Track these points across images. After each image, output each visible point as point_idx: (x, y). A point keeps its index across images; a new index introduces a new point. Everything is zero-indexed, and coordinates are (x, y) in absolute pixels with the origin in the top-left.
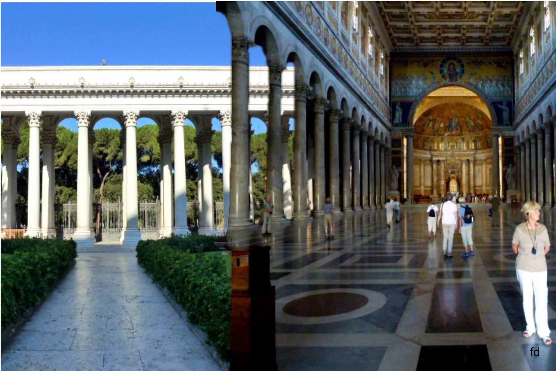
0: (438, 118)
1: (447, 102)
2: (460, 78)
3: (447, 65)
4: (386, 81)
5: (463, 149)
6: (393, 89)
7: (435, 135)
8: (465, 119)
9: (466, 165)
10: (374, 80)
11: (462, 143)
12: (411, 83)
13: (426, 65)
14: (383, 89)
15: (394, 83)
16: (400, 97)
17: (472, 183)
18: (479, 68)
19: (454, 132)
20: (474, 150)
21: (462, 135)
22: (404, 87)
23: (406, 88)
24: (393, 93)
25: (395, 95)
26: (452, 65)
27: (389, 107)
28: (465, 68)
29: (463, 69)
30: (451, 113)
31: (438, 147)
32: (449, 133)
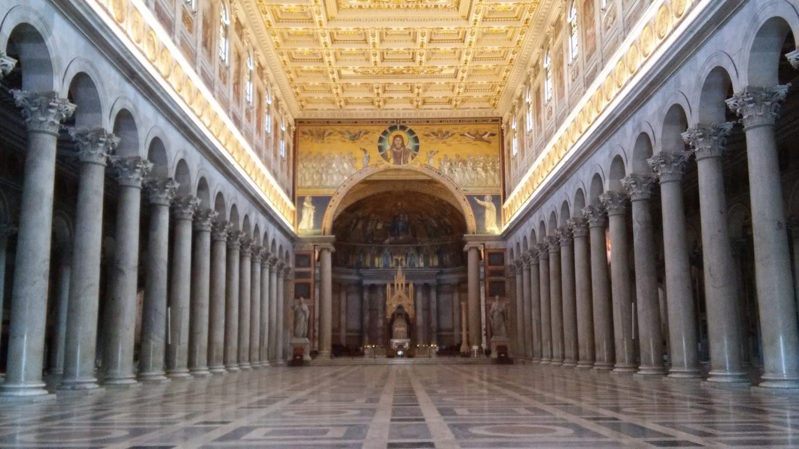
0: (373, 215)
1: (390, 188)
3: (391, 138)
4: (288, 164)
5: (417, 266)
7: (366, 242)
10: (272, 167)
12: (329, 165)
13: (354, 138)
15: (300, 166)
16: (309, 187)
17: (434, 323)
18: (446, 143)
19: (401, 238)
20: (437, 267)
21: (416, 242)
23: (321, 174)
24: (299, 183)
25: (303, 185)
26: (398, 139)
28: (422, 142)
29: (416, 144)
30: (396, 206)
31: (373, 263)
32: (392, 238)
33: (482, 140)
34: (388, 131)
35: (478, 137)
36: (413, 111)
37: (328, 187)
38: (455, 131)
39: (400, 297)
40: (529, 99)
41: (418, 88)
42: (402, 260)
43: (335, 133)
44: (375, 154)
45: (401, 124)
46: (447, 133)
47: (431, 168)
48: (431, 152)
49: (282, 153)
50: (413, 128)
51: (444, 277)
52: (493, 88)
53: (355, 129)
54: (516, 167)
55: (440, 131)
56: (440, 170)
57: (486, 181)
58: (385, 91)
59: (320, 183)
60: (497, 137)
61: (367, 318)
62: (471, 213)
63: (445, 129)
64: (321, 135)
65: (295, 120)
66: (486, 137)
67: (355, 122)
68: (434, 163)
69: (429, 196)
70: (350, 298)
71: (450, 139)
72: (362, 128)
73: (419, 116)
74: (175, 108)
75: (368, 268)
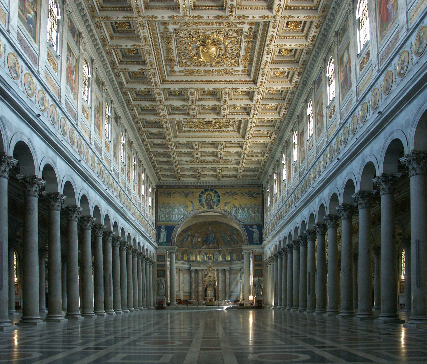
1: (205, 220)
2: (217, 206)
5: (219, 260)
6: (159, 215)
7: (193, 248)
8: (222, 234)
9: (222, 274)
11: (219, 256)
12: (173, 209)
13: (187, 195)
14: (151, 218)
15: (159, 210)
16: (164, 221)
18: (234, 198)
19: (211, 246)
22: (168, 213)
23: (170, 214)
26: (209, 196)
27: (155, 230)
30: (208, 229)
31: (196, 258)
32: (206, 246)
33: (253, 197)
34: (204, 191)
35: (251, 195)
36: (217, 181)
37: (173, 221)
38: (239, 192)
39: (210, 277)
40: (275, 177)
41: (219, 170)
42: (211, 257)
43: (177, 193)
44: (197, 204)
45: (211, 188)
46: (235, 192)
47: (226, 211)
48: (226, 203)
49: (150, 203)
50: (217, 190)
51: (233, 266)
52: (258, 170)
53: (187, 191)
54: (269, 212)
55: (231, 192)
56: (231, 212)
57: (254, 218)
58: (202, 171)
59: (169, 219)
60: (260, 195)
61: (193, 286)
62: (247, 235)
63: (233, 191)
64: (169, 194)
65: (156, 186)
66: (254, 195)
67: (187, 187)
68: (227, 208)
69: (226, 224)
70: (184, 276)
71: (236, 196)
72: (190, 190)
73: (220, 184)
74: (97, 184)
75: (193, 261)
